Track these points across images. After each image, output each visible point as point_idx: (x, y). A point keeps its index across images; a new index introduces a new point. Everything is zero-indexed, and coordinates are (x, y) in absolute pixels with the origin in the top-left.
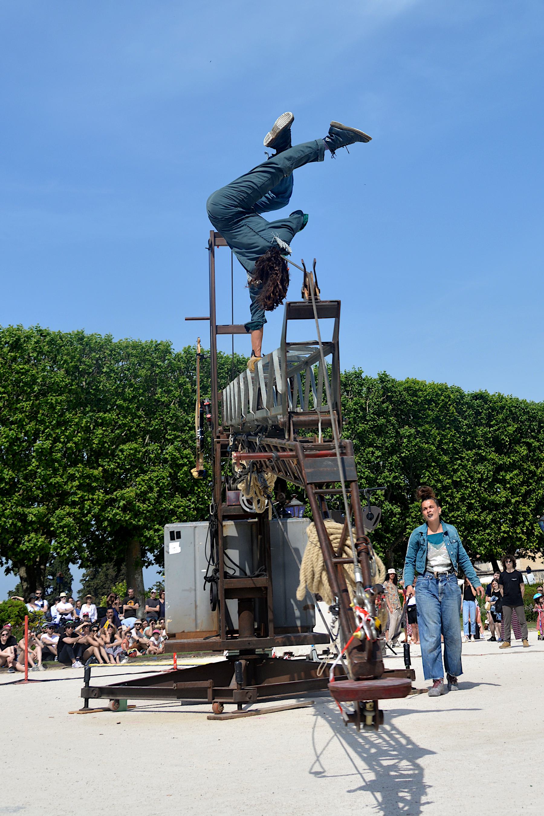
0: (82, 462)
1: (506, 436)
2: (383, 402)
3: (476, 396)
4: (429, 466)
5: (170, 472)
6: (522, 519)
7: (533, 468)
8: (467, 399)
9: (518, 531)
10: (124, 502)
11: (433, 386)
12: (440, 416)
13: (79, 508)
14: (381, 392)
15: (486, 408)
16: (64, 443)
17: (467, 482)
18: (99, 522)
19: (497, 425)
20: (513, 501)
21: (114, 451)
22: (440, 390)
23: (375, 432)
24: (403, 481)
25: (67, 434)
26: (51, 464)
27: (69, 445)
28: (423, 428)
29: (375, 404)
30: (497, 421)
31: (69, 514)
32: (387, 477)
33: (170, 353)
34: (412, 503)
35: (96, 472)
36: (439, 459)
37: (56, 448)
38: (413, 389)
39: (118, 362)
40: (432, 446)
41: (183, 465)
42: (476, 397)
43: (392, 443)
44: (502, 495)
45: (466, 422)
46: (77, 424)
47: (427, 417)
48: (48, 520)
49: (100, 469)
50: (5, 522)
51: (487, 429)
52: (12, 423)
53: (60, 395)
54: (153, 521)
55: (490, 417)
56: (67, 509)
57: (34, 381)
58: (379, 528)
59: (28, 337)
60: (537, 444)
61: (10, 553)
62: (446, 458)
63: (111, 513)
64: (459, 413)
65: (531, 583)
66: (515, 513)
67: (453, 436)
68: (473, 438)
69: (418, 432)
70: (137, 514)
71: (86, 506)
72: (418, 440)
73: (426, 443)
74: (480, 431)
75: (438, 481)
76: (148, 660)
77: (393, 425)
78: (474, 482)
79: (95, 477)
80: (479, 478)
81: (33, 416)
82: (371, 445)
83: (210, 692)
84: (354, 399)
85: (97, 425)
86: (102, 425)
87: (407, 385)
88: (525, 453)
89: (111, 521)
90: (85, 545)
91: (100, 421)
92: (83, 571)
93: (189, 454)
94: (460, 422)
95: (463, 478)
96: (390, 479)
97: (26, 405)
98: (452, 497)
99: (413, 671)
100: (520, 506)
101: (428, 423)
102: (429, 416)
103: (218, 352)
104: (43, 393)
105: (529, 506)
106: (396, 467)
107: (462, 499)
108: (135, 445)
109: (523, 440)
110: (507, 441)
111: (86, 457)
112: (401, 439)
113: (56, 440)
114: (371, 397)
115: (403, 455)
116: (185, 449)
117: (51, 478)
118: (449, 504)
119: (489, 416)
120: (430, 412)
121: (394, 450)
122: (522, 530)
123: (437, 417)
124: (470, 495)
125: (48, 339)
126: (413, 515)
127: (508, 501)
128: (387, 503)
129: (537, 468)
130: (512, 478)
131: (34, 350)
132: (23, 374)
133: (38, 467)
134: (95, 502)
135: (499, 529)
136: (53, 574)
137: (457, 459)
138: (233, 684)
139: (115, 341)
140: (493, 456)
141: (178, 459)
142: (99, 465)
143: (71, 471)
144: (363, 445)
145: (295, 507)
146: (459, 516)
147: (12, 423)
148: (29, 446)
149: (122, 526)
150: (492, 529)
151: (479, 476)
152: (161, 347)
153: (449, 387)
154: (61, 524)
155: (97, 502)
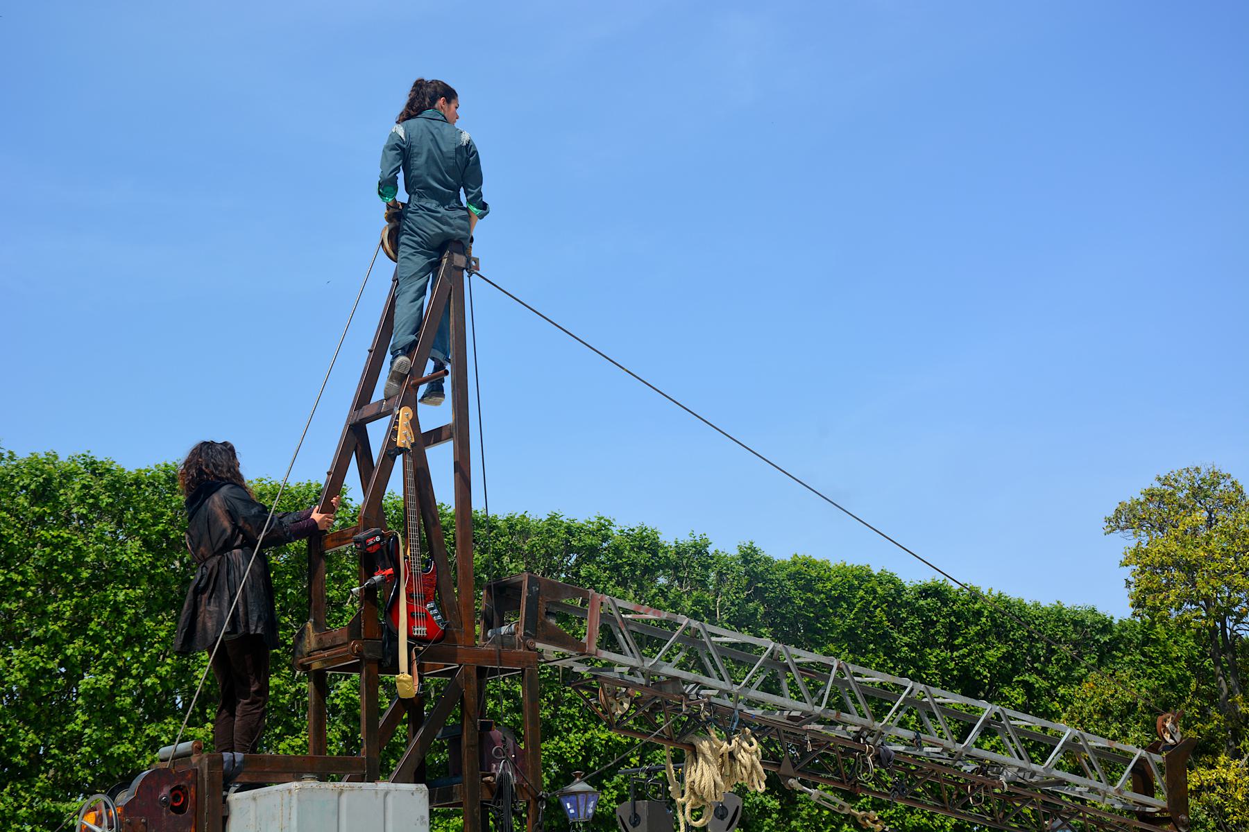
1: (984, 666)
2: (748, 600)
3: (925, 590)
5: (343, 732)
11: (843, 572)
12: (857, 628)
14: (745, 582)
19: (965, 645)
22: (856, 577)
25: (144, 660)
27: (148, 682)
29: (733, 604)
30: (965, 638)
37: (123, 688)
38: (805, 576)
42: (925, 592)
45: (906, 639)
47: (831, 630)
52: (37, 641)
53: (132, 587)
55: (952, 631)
59: (68, 476)
60: (1046, 684)
64: (893, 622)
68: (919, 669)
84: (695, 593)
87: (793, 569)
101: (834, 641)
102: (836, 627)
104: (97, 583)
110: (986, 677)
111: (180, 706)
113: (123, 673)
114: (724, 590)
117: (110, 746)
119: (951, 630)
120: (837, 621)
123: (850, 629)
125: (107, 479)
131: (81, 500)
132: (56, 547)
133: (86, 724)
143: (151, 730)
145: (580, 797)
146: (891, 817)
147: (37, 641)
148: (68, 685)
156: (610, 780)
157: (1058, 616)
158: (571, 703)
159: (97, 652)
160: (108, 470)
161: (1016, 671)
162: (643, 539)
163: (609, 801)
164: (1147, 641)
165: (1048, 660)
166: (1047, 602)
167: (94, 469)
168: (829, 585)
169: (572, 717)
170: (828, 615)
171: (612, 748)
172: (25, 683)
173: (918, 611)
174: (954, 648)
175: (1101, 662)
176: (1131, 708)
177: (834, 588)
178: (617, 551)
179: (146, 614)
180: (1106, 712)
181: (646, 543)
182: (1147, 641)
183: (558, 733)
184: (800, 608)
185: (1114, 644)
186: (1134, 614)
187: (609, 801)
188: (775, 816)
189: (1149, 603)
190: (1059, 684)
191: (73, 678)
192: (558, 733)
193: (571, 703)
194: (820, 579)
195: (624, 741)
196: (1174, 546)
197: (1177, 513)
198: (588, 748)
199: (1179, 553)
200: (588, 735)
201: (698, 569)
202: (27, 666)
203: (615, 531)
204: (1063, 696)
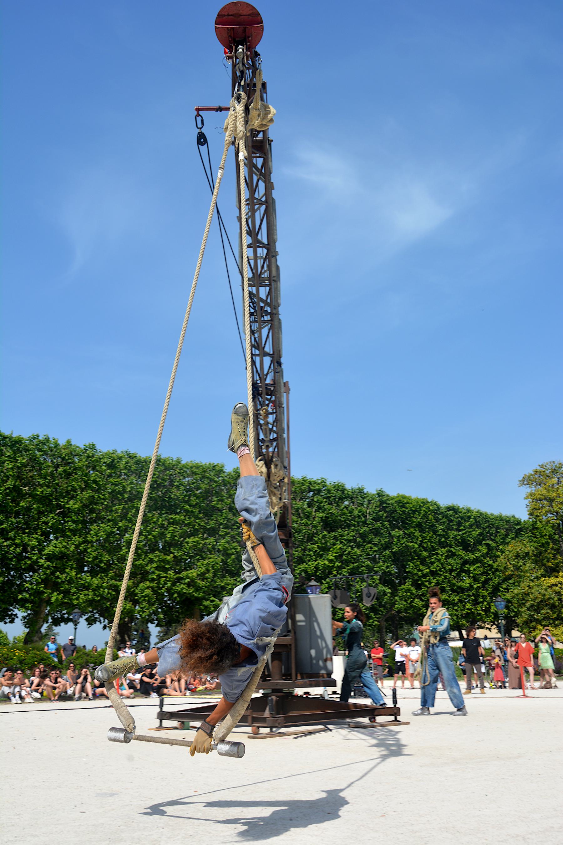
0: (158, 550)
1: (471, 538)
2: (380, 511)
3: (449, 508)
6: (481, 600)
7: (491, 562)
9: (478, 609)
10: (189, 580)
11: (417, 500)
14: (378, 504)
15: (456, 517)
17: (441, 571)
18: (171, 595)
19: (464, 530)
20: (475, 586)
21: (182, 542)
22: (422, 503)
23: (373, 533)
24: (393, 569)
25: (148, 529)
27: (150, 537)
28: (409, 531)
31: (148, 587)
33: (224, 472)
35: (168, 558)
36: (420, 554)
38: (402, 502)
39: (185, 478)
40: (415, 545)
41: (233, 554)
43: (385, 542)
44: (467, 582)
46: (154, 523)
47: (412, 523)
48: (134, 591)
50: (103, 592)
51: (457, 533)
52: (109, 520)
54: (209, 594)
55: (459, 524)
57: (124, 491)
58: (375, 604)
59: (120, 459)
60: (494, 545)
61: (106, 615)
62: (425, 554)
63: (179, 587)
65: (487, 647)
66: (477, 595)
67: (431, 537)
69: (405, 534)
70: (198, 589)
72: (405, 539)
73: (412, 542)
74: (452, 534)
76: (205, 694)
77: (387, 528)
79: (167, 561)
82: (370, 542)
83: (250, 719)
84: (359, 508)
85: (170, 523)
86: (173, 523)
87: (397, 499)
88: (485, 552)
89: (179, 593)
90: (160, 610)
92: (159, 629)
93: (236, 546)
97: (119, 508)
98: (430, 583)
99: (399, 709)
100: (481, 591)
101: (413, 527)
102: (414, 522)
105: (487, 590)
106: (388, 559)
107: (437, 584)
108: (197, 539)
109: (484, 542)
112: (392, 538)
115: (393, 550)
116: (234, 542)
119: (459, 523)
120: (414, 520)
121: (387, 547)
122: (482, 608)
123: (420, 523)
124: (443, 582)
125: (135, 460)
126: (400, 594)
127: (471, 586)
128: (381, 585)
129: (494, 562)
130: (474, 570)
131: (125, 468)
132: (116, 485)
135: (464, 606)
136: (137, 631)
137: (434, 554)
138: (267, 714)
139: (183, 462)
141: (228, 550)
142: (171, 553)
143: (151, 556)
144: (364, 542)
147: (109, 520)
149: (187, 597)
150: (458, 607)
151: (450, 567)
152: (217, 468)
153: (429, 501)
156: (325, 580)
157: (500, 518)
158: (310, 550)
160: (135, 457)
161: (484, 540)
162: (339, 487)
165: (496, 536)
166: (496, 513)
167: (130, 456)
168: (411, 505)
169: (310, 555)
170: (410, 517)
171: (325, 568)
172: (105, 537)
173: (446, 516)
174: (460, 531)
175: (516, 536)
176: (527, 554)
177: (413, 506)
178: (329, 491)
180: (518, 556)
181: (340, 488)
182: (534, 528)
183: (305, 562)
184: (400, 514)
185: (520, 530)
189: (535, 514)
191: (122, 536)
192: (305, 562)
193: (310, 550)
195: (331, 565)
198: (317, 568)
199: (547, 494)
200: (316, 563)
201: (360, 499)
202: (106, 530)
203: (328, 483)
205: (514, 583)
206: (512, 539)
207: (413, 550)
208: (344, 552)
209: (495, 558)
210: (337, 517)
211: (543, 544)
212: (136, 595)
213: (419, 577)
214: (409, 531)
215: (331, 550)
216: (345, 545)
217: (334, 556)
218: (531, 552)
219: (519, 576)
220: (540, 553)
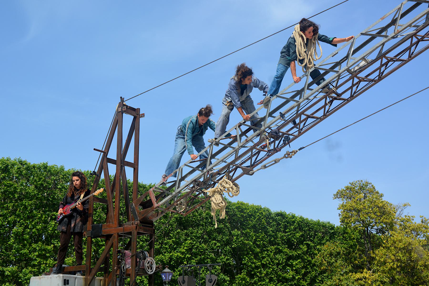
0: (41, 240)
1: (295, 238)
3: (278, 214)
4: (248, 254)
5: (94, 249)
7: (310, 259)
8: (273, 216)
11: (253, 207)
13: (37, 269)
15: (283, 221)
16: (31, 229)
17: (270, 265)
19: (289, 232)
20: (297, 278)
22: (257, 209)
24: (232, 262)
26: (22, 241)
28: (246, 231)
30: (290, 230)
32: (223, 259)
34: (237, 274)
36: (254, 250)
40: (250, 242)
42: (278, 214)
43: (227, 239)
44: (290, 274)
47: (248, 225)
49: (52, 245)
53: (31, 200)
55: (286, 227)
56: (30, 268)
57: (15, 192)
59: (13, 165)
60: (312, 244)
62: (258, 250)
64: (267, 223)
67: (263, 237)
68: (275, 238)
69: (242, 233)
71: (42, 267)
72: (242, 238)
73: (247, 240)
74: (280, 234)
75: (253, 263)
77: (228, 228)
78: (274, 265)
79: (48, 250)
80: (277, 263)
81: (13, 212)
82: (214, 239)
84: (207, 211)
88: (305, 250)
91: (54, 217)
94: (268, 229)
95: (267, 262)
96: (225, 260)
98: (260, 273)
101: (249, 228)
102: (250, 224)
103: (127, 179)
106: (228, 253)
107: (267, 274)
110: (295, 242)
112: (233, 237)
113: (26, 227)
115: (233, 246)
117: (21, 250)
118: (259, 277)
120: (250, 222)
123: (254, 225)
124: (271, 273)
125: (25, 166)
126: (237, 282)
127: (294, 278)
128: (222, 274)
129: (312, 259)
130: (296, 264)
132: (8, 187)
133: (14, 243)
134: (47, 265)
139: (66, 169)
140: (286, 250)
142: (52, 244)
143: (34, 246)
144: (209, 239)
145: (167, 274)
148: (10, 230)
151: (277, 261)
154: (26, 278)
155: (49, 265)
156: (177, 269)
157: (318, 224)
158: (166, 244)
159: (18, 220)
160: (26, 164)
161: (304, 240)
163: (176, 275)
164: (345, 233)
165: (314, 238)
166: (315, 219)
167: (21, 163)
168: (248, 211)
169: (166, 248)
170: (247, 220)
171: (178, 258)
174: (286, 232)
175: (330, 238)
176: (339, 253)
177: (250, 212)
179: (34, 209)
180: (331, 254)
182: (345, 233)
183: (162, 253)
184: (239, 218)
185: (334, 234)
186: (341, 225)
187: (176, 275)
188: (228, 282)
189: (346, 221)
190: (317, 245)
191: (11, 229)
192: (162, 253)
193: (166, 244)
194: (246, 209)
195: (182, 256)
196: (354, 204)
197: (355, 194)
198: (171, 258)
199: (355, 206)
200: (171, 254)
204: (318, 249)
205: (328, 277)
206: (327, 240)
207: (248, 247)
208: (194, 246)
209: (313, 255)
210: (189, 217)
211: (351, 245)
212: (20, 278)
213: (252, 268)
214: (246, 231)
215: (183, 244)
216: (195, 240)
217: (186, 250)
218: (342, 252)
219: (332, 271)
220: (349, 253)
